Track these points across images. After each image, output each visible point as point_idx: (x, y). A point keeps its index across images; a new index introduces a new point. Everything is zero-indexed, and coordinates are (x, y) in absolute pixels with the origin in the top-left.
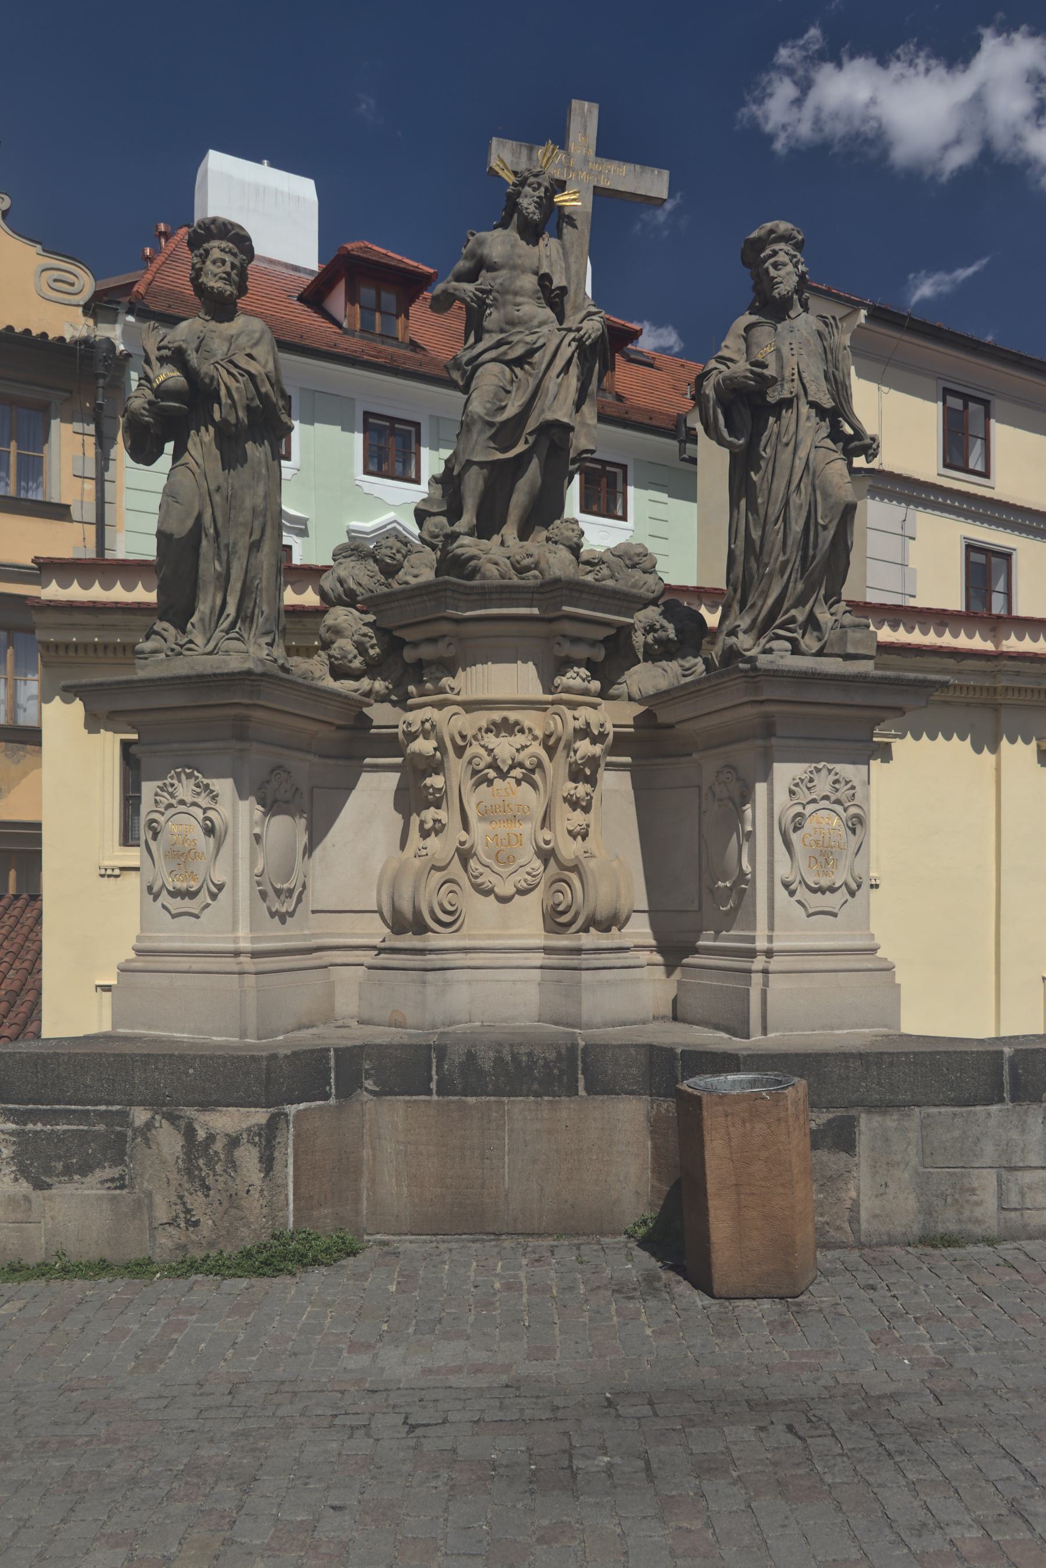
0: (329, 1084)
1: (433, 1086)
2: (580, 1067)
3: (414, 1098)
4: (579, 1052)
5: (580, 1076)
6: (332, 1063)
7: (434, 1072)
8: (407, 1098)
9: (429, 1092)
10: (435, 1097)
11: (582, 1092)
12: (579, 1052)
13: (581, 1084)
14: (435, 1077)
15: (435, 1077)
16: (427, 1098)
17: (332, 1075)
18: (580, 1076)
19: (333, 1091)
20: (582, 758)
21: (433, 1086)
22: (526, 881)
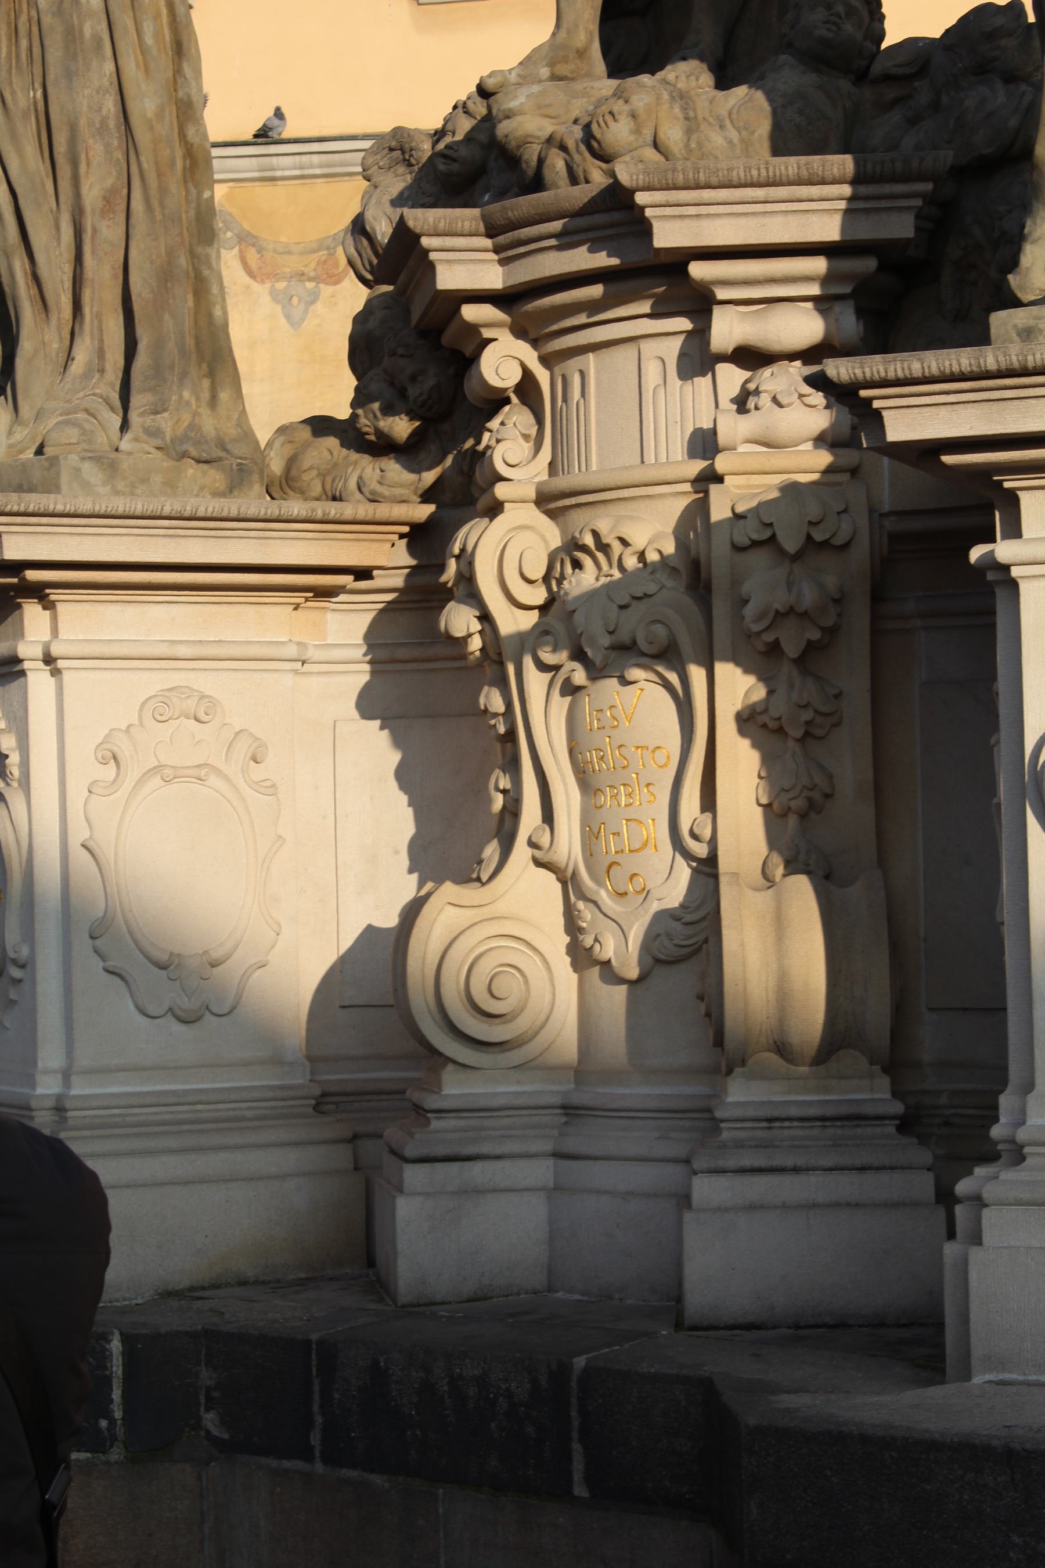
0: (108, 1415)
1: (315, 1439)
2: (576, 1424)
3: (287, 1464)
4: (574, 1384)
5: (577, 1447)
6: (117, 1367)
7: (316, 1408)
8: (273, 1463)
9: (307, 1455)
10: (319, 1467)
11: (580, 1490)
12: (574, 1384)
13: (578, 1465)
14: (319, 1419)
15: (319, 1419)
16: (299, 1465)
17: (117, 1394)
18: (577, 1447)
19: (120, 1431)
20: (759, 618)
21: (315, 1439)
22: (669, 936)
